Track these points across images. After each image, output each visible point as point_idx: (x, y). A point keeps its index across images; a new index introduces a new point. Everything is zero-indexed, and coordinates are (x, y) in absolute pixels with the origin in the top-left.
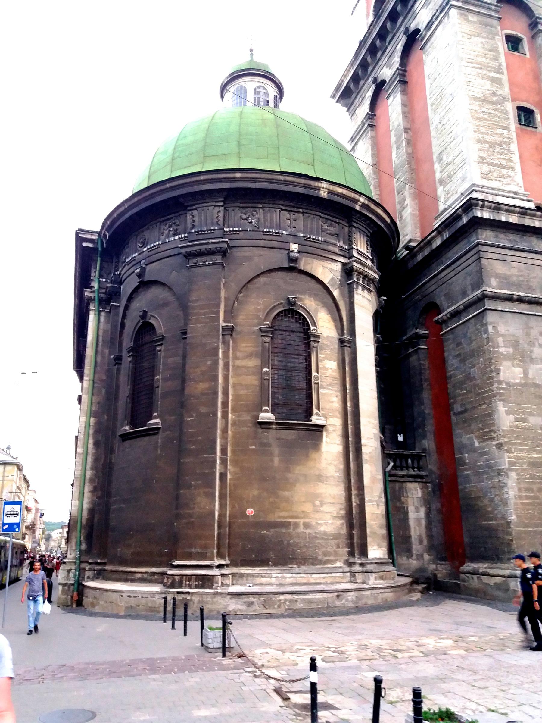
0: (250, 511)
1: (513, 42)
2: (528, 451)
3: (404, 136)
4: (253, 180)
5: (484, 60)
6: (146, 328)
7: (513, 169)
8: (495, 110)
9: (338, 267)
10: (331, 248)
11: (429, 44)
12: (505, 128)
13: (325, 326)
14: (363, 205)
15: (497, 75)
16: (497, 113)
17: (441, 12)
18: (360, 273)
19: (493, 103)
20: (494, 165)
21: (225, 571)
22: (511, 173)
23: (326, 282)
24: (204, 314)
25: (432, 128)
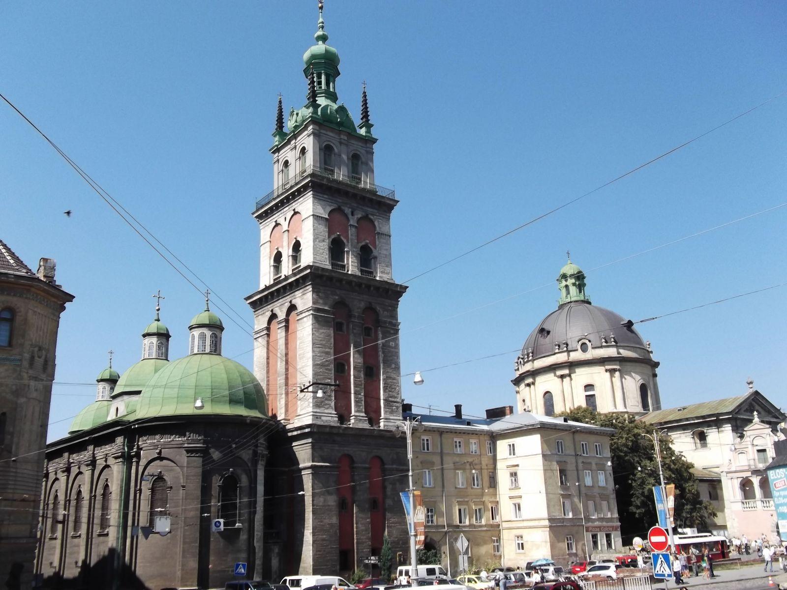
1: (338, 327)
2: (322, 535)
5: (324, 342)
6: (160, 478)
7: (330, 400)
8: (327, 369)
9: (251, 452)
11: (300, 321)
12: (329, 379)
13: (244, 481)
14: (265, 422)
15: (329, 350)
16: (327, 371)
17: (308, 311)
18: (260, 454)
19: (325, 366)
22: (330, 402)
23: (246, 460)
24: (194, 479)
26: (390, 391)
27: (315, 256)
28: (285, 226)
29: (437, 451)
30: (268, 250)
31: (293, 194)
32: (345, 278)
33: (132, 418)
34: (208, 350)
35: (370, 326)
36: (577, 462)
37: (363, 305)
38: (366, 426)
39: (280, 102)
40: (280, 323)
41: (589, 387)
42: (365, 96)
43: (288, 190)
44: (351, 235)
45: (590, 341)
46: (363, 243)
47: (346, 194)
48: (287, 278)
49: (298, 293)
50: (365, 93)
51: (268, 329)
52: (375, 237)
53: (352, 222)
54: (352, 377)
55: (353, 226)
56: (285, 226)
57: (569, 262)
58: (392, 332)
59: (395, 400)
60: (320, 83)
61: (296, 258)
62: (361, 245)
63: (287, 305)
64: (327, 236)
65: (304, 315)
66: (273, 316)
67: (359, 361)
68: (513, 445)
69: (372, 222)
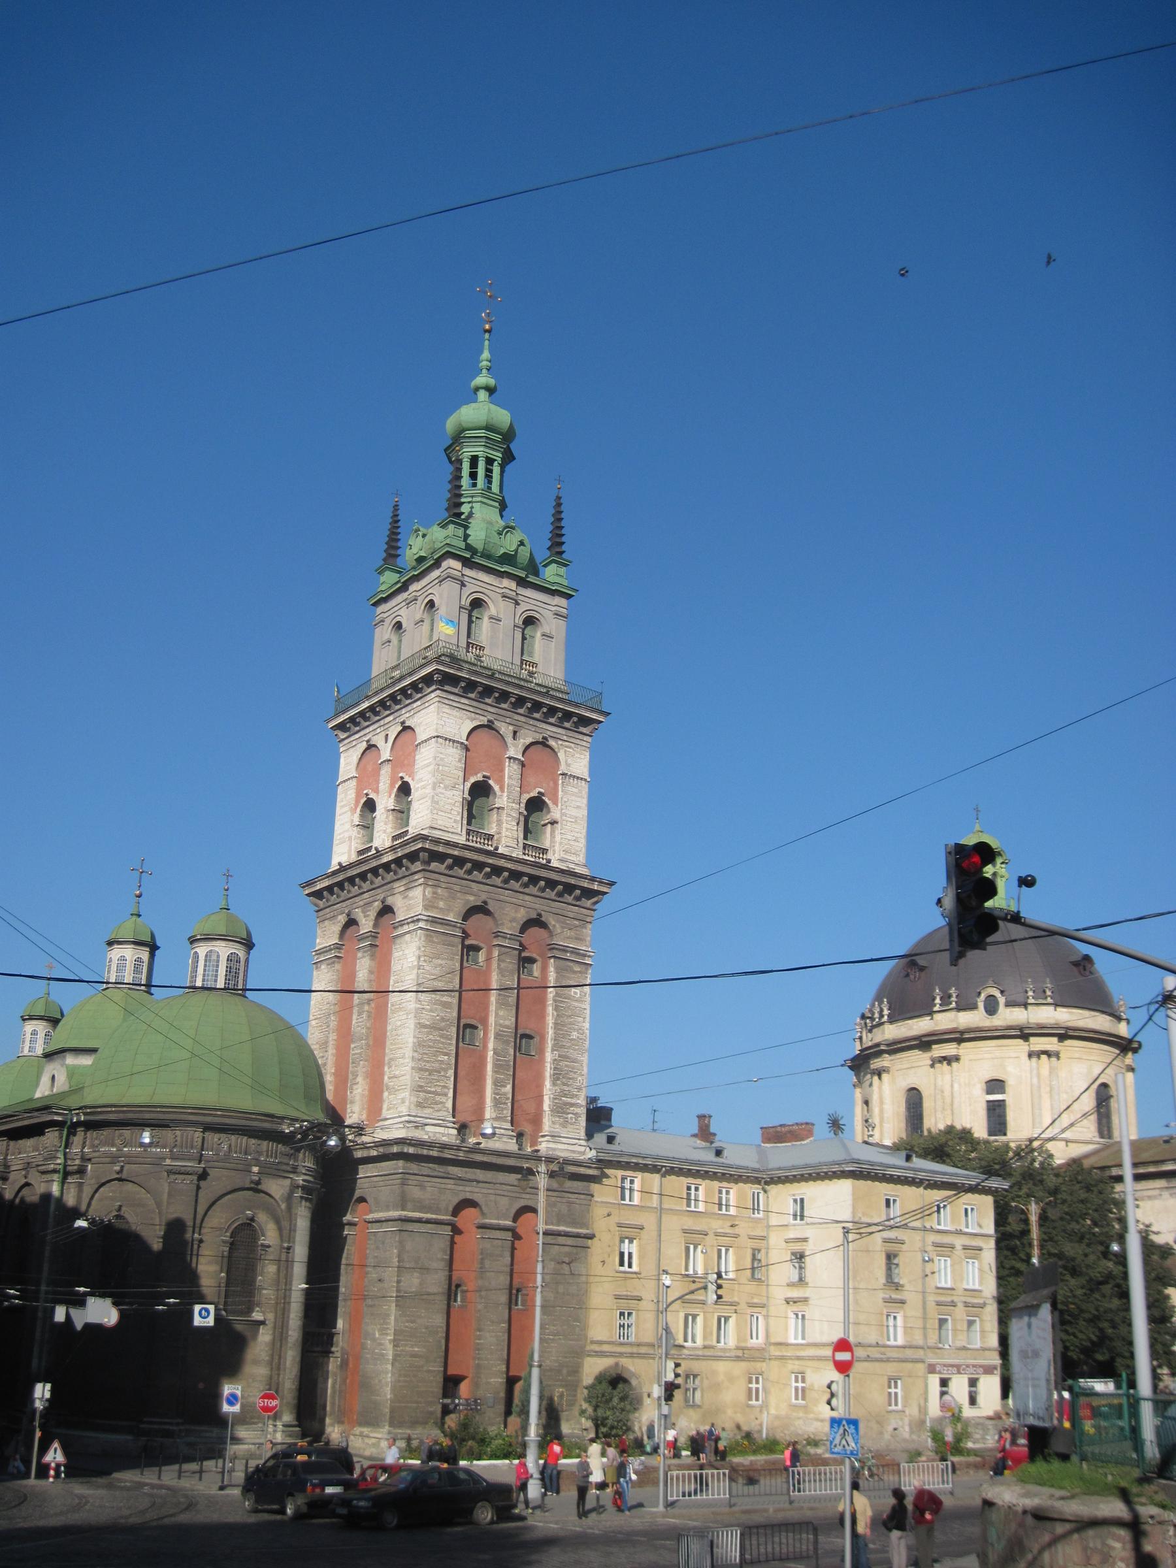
0: (201, 1386)
2: (412, 1346)
3: (366, 1008)
4: (229, 1117)
8: (441, 1036)
9: (287, 1182)
10: (284, 1167)
11: (398, 941)
13: (270, 1235)
15: (449, 1000)
20: (430, 1092)
21: (182, 1428)
22: (443, 1099)
23: (277, 1197)
25: (389, 1028)
26: (564, 1084)
27: (435, 816)
28: (386, 754)
29: (649, 1204)
30: (352, 794)
31: (403, 691)
32: (490, 861)
33: (74, 1102)
34: (221, 984)
35: (534, 955)
36: (924, 1241)
37: (522, 915)
38: (512, 1146)
39: (396, 507)
40: (362, 938)
41: (995, 1085)
42: (559, 505)
43: (393, 684)
44: (510, 777)
45: (1002, 992)
46: (534, 794)
47: (504, 696)
48: (379, 854)
49: (399, 886)
50: (558, 498)
51: (338, 947)
52: (556, 784)
53: (511, 752)
54: (490, 1054)
55: (515, 759)
56: (386, 754)
57: (977, 827)
58: (577, 968)
59: (573, 1101)
60: (473, 476)
61: (402, 813)
62: (526, 797)
63: (377, 905)
64: (461, 780)
65: (406, 928)
66: (351, 922)
67: (507, 1023)
68: (802, 1200)
69: (556, 753)
